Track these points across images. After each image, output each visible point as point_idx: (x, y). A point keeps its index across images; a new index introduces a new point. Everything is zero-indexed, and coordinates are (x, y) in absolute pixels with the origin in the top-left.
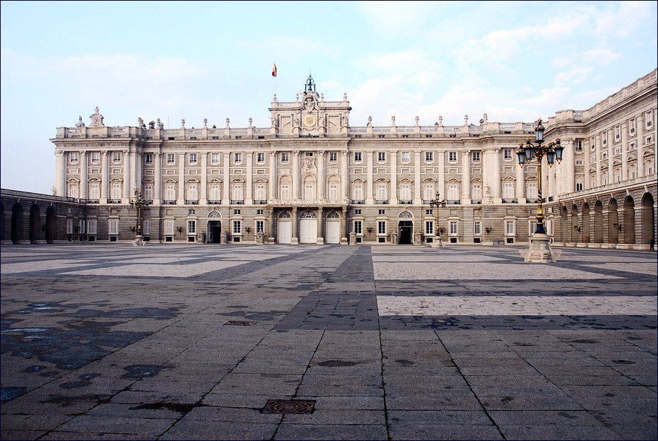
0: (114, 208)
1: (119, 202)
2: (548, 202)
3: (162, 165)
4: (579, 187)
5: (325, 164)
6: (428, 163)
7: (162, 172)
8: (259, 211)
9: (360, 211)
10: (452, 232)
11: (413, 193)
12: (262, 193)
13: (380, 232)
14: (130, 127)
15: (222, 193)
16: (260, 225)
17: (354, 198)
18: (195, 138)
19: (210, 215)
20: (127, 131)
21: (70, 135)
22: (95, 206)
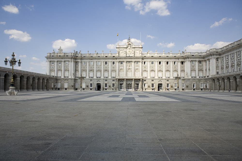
0: (66, 79)
1: (68, 77)
3: (81, 65)
4: (218, 73)
7: (81, 67)
8: (113, 80)
9: (146, 80)
10: (175, 87)
11: (162, 75)
13: (152, 87)
14: (71, 53)
15: (101, 74)
16: (113, 85)
18: (92, 57)
21: (52, 56)
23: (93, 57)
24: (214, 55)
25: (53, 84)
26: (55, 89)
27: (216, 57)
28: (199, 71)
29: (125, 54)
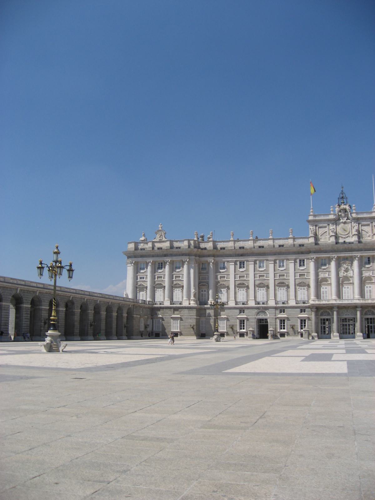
5: (361, 266)
12: (304, 294)
16: (303, 321)
18: (243, 248)
19: (258, 313)
23: (246, 249)
25: (143, 322)
26: (149, 336)
29: (331, 237)
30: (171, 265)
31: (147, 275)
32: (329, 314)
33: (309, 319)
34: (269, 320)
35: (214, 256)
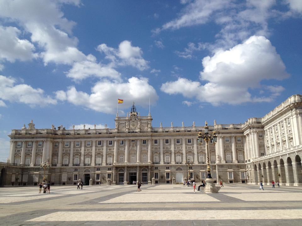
2: (248, 162)
4: (262, 154)
6: (189, 144)
7: (63, 150)
9: (157, 167)
16: (109, 175)
17: (154, 161)
18: (79, 134)
20: (46, 131)
22: (28, 168)
24: (253, 128)
27: (258, 130)
28: (237, 152)
30: (36, 143)
31: (21, 150)
32: (123, 171)
33: (112, 173)
34: (90, 175)
35: (62, 138)
